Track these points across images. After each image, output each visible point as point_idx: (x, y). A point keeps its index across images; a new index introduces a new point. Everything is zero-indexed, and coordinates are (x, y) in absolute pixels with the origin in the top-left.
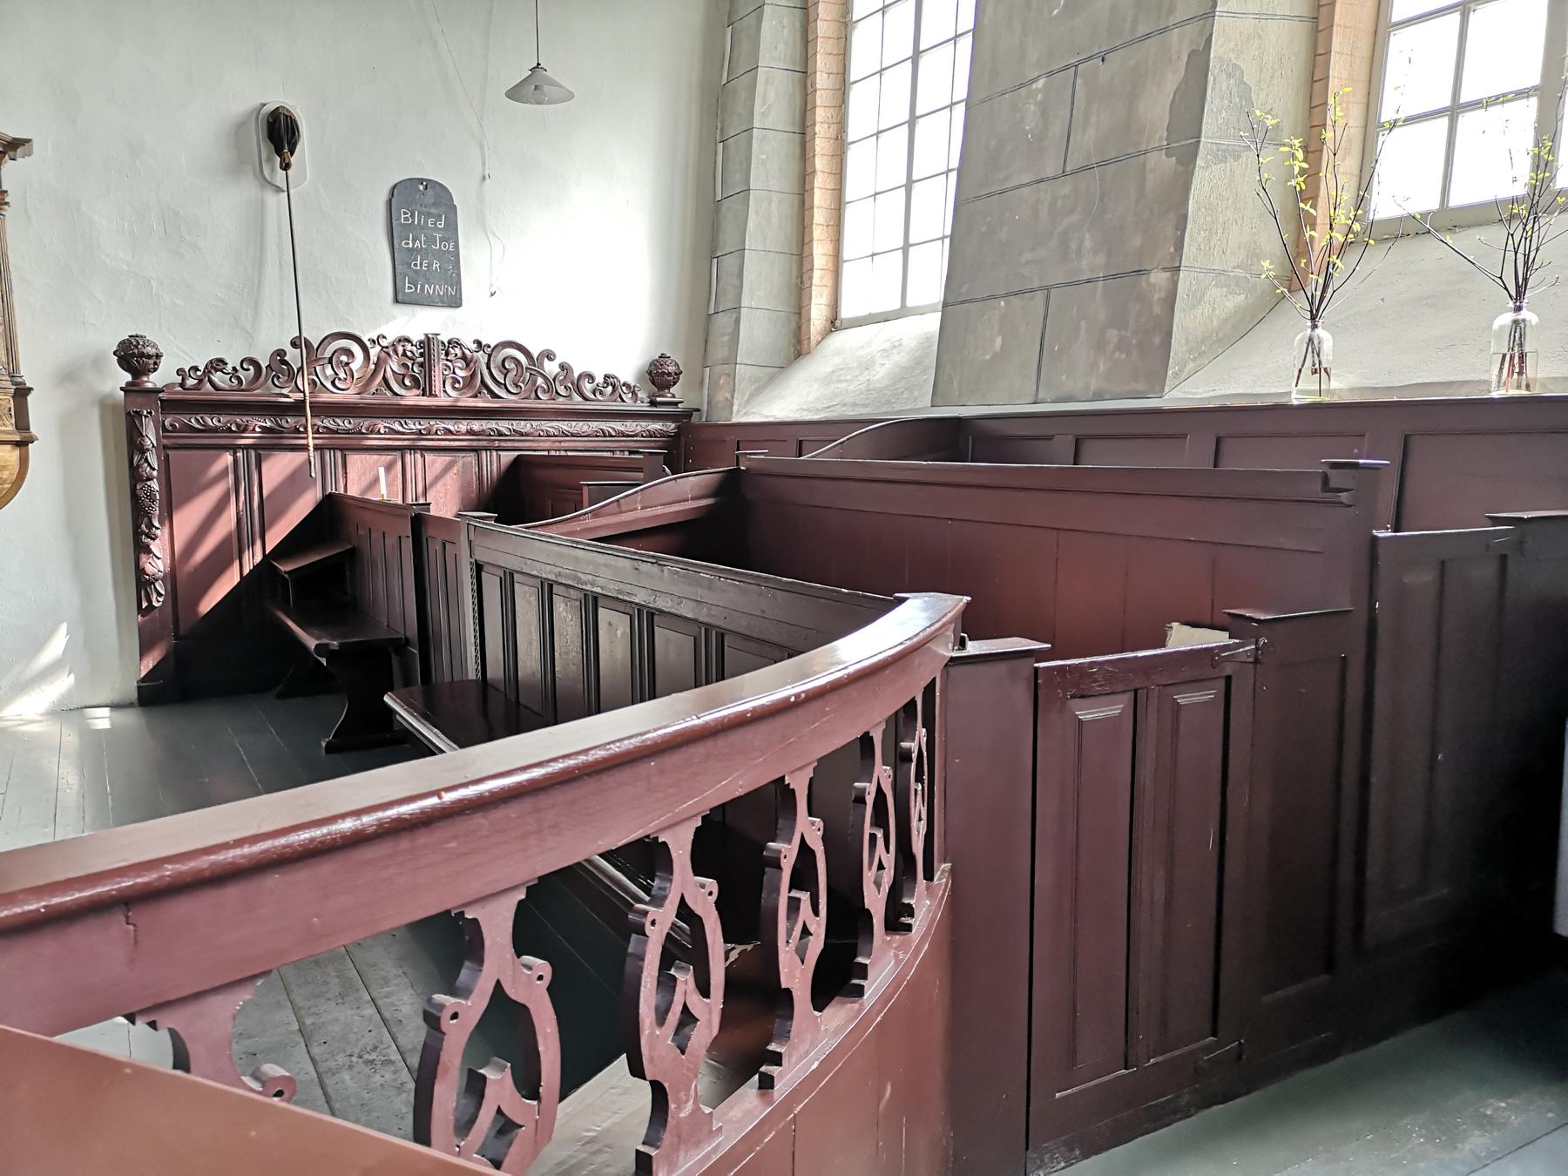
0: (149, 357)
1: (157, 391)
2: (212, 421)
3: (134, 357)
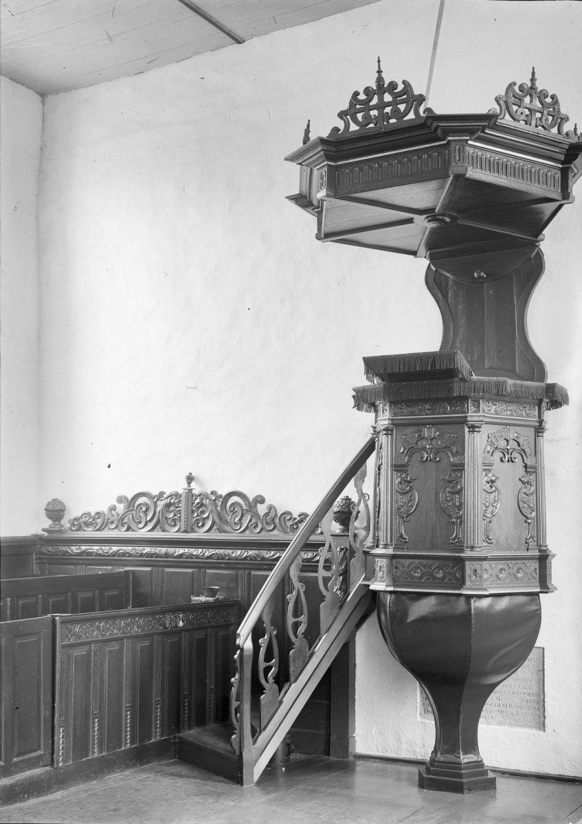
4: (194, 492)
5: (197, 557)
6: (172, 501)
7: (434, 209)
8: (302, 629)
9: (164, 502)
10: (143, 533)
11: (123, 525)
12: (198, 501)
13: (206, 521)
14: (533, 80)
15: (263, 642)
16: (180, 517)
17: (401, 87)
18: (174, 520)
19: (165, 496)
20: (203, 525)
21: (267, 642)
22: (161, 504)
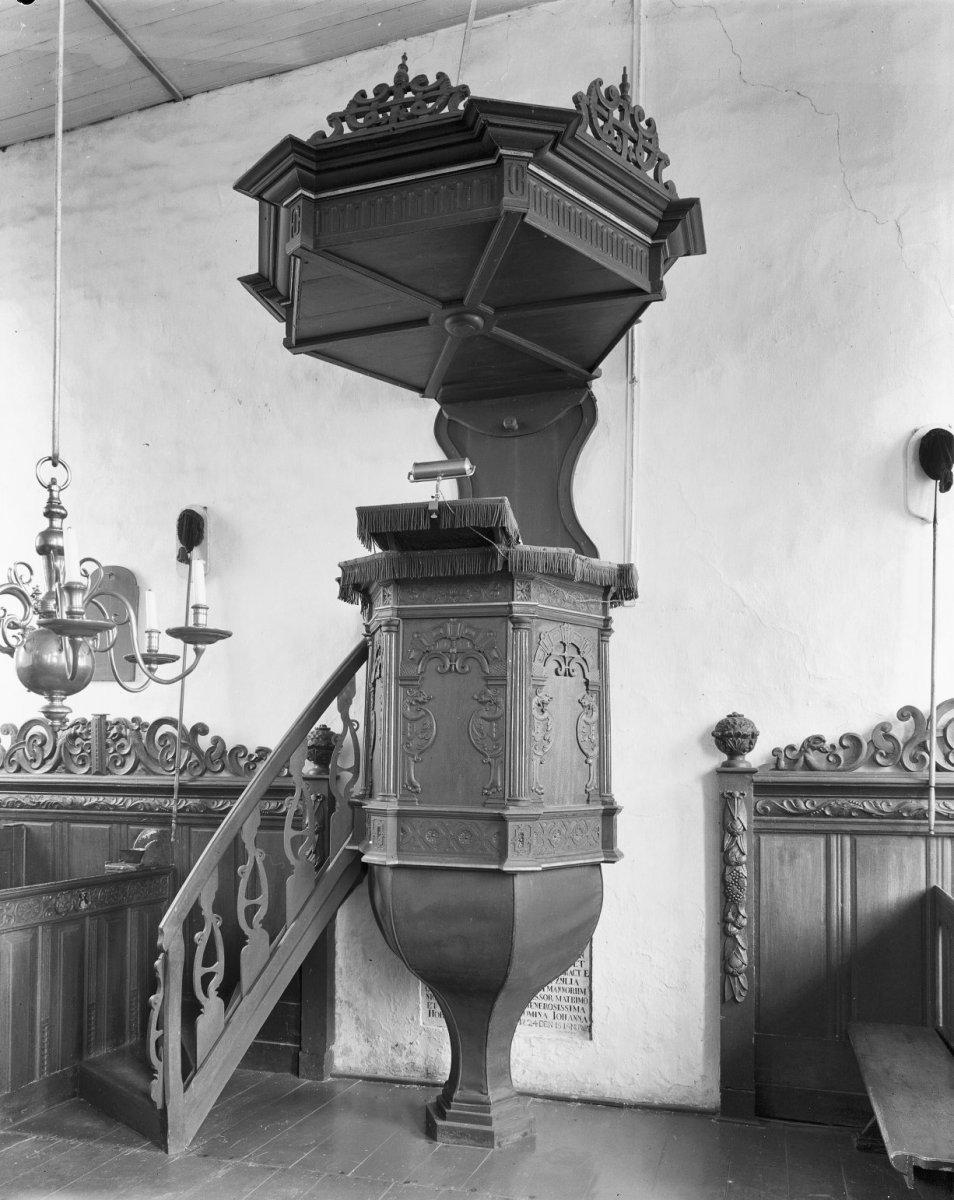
0: (745, 736)
1: (752, 772)
2: (804, 805)
3: (730, 737)
4: (108, 719)
5: (116, 808)
6: (78, 731)
7: (461, 300)
8: (261, 914)
9: (67, 732)
10: (38, 775)
11: (11, 764)
12: (114, 731)
13: (128, 759)
14: (624, 86)
15: (201, 938)
16: (90, 753)
17: (432, 80)
18: (82, 758)
19: (68, 724)
20: (123, 765)
21: (206, 937)
22: (62, 735)
